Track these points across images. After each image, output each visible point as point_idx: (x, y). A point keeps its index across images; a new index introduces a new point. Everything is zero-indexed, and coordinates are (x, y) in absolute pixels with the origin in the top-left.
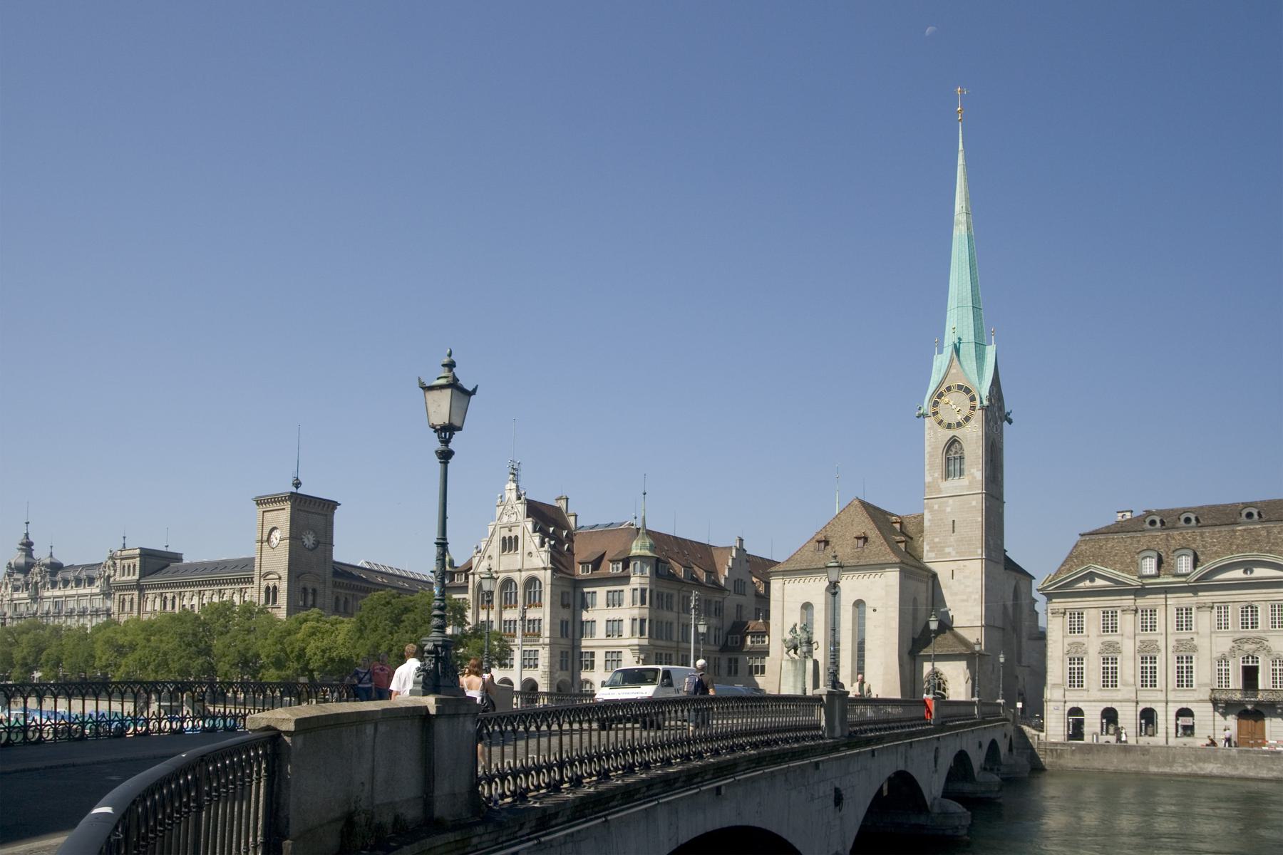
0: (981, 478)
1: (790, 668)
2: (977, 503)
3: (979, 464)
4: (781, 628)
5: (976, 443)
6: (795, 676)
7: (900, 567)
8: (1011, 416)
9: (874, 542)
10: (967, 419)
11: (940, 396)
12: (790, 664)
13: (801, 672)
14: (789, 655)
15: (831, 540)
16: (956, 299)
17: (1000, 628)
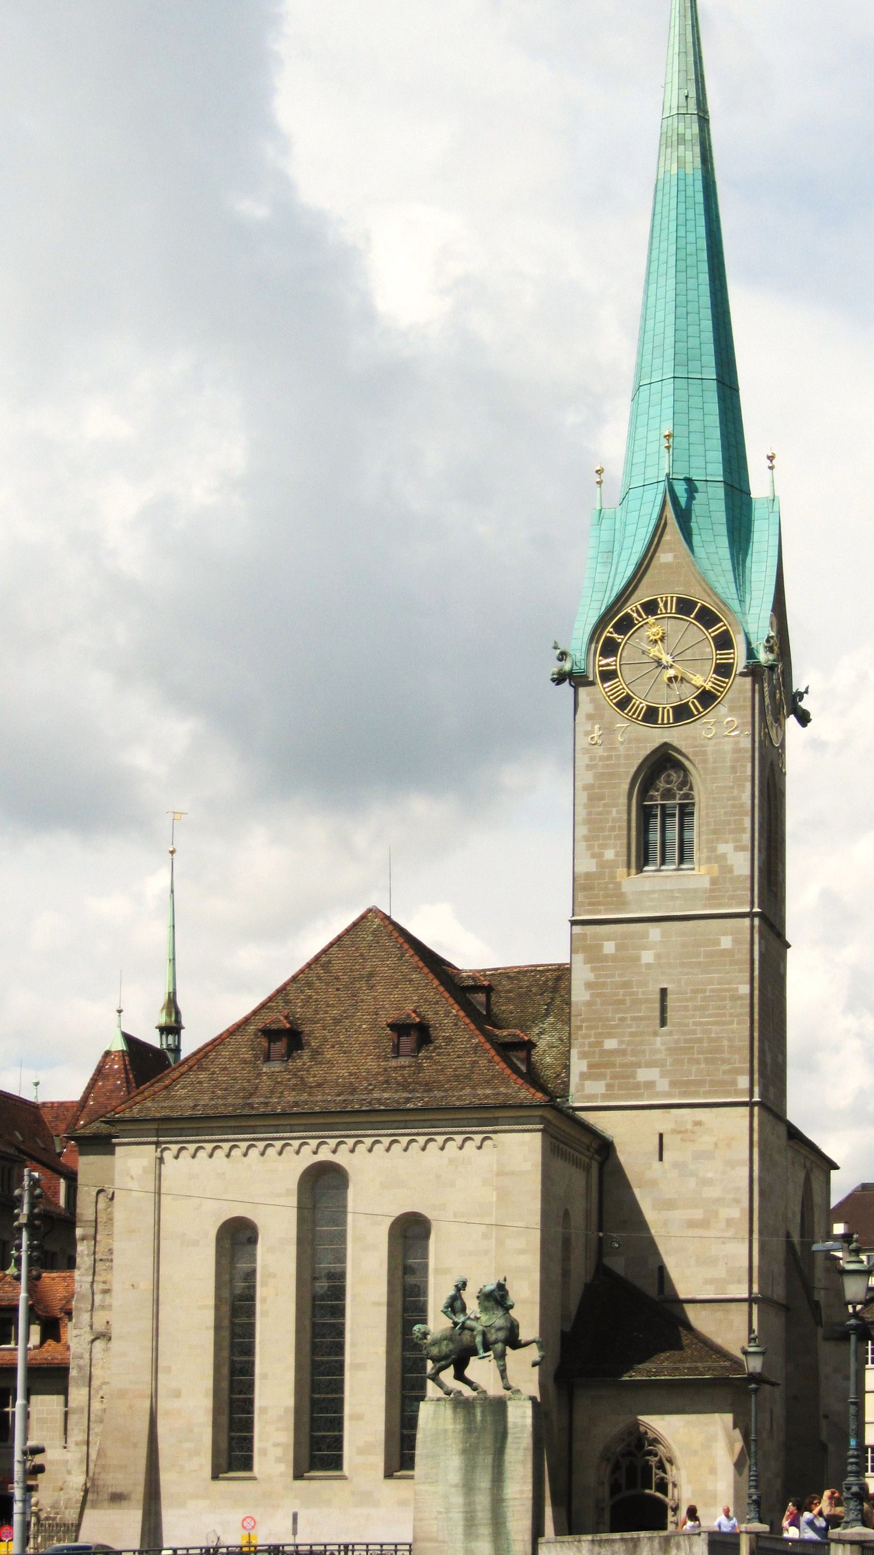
0: (747, 872)
1: (450, 1426)
2: (736, 941)
3: (743, 830)
4: (149, 1297)
5: (734, 769)
6: (469, 1452)
7: (543, 1120)
8: (804, 704)
9: (449, 1040)
10: (707, 698)
11: (625, 625)
12: (447, 1412)
13: (488, 1440)
14: (440, 1385)
15: (306, 1028)
16: (670, 352)
17: (778, 1304)
